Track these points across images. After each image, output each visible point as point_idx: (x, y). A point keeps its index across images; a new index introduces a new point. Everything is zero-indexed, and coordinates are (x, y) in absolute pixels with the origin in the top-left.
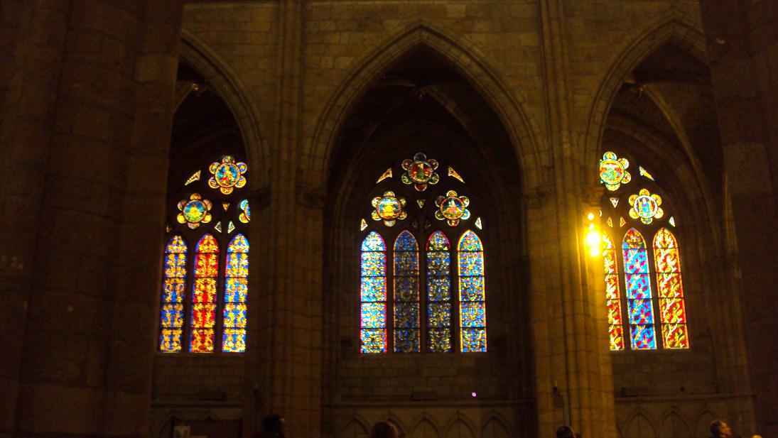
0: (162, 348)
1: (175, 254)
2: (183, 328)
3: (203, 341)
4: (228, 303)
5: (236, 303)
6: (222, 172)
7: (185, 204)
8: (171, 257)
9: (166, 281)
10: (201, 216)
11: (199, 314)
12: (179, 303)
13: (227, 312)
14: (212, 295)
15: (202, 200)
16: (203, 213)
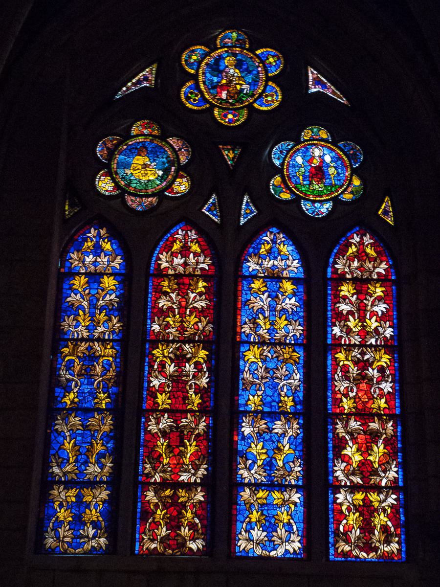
0: (50, 542)
1: (87, 274)
2: (114, 482)
3: (174, 524)
4: (246, 413)
5: (273, 416)
6: (216, 68)
7: (116, 146)
8: (79, 282)
9: (66, 350)
10: (162, 178)
11: (162, 445)
12: (100, 411)
13: (244, 438)
14: (198, 390)
15: (163, 137)
16: (166, 171)
